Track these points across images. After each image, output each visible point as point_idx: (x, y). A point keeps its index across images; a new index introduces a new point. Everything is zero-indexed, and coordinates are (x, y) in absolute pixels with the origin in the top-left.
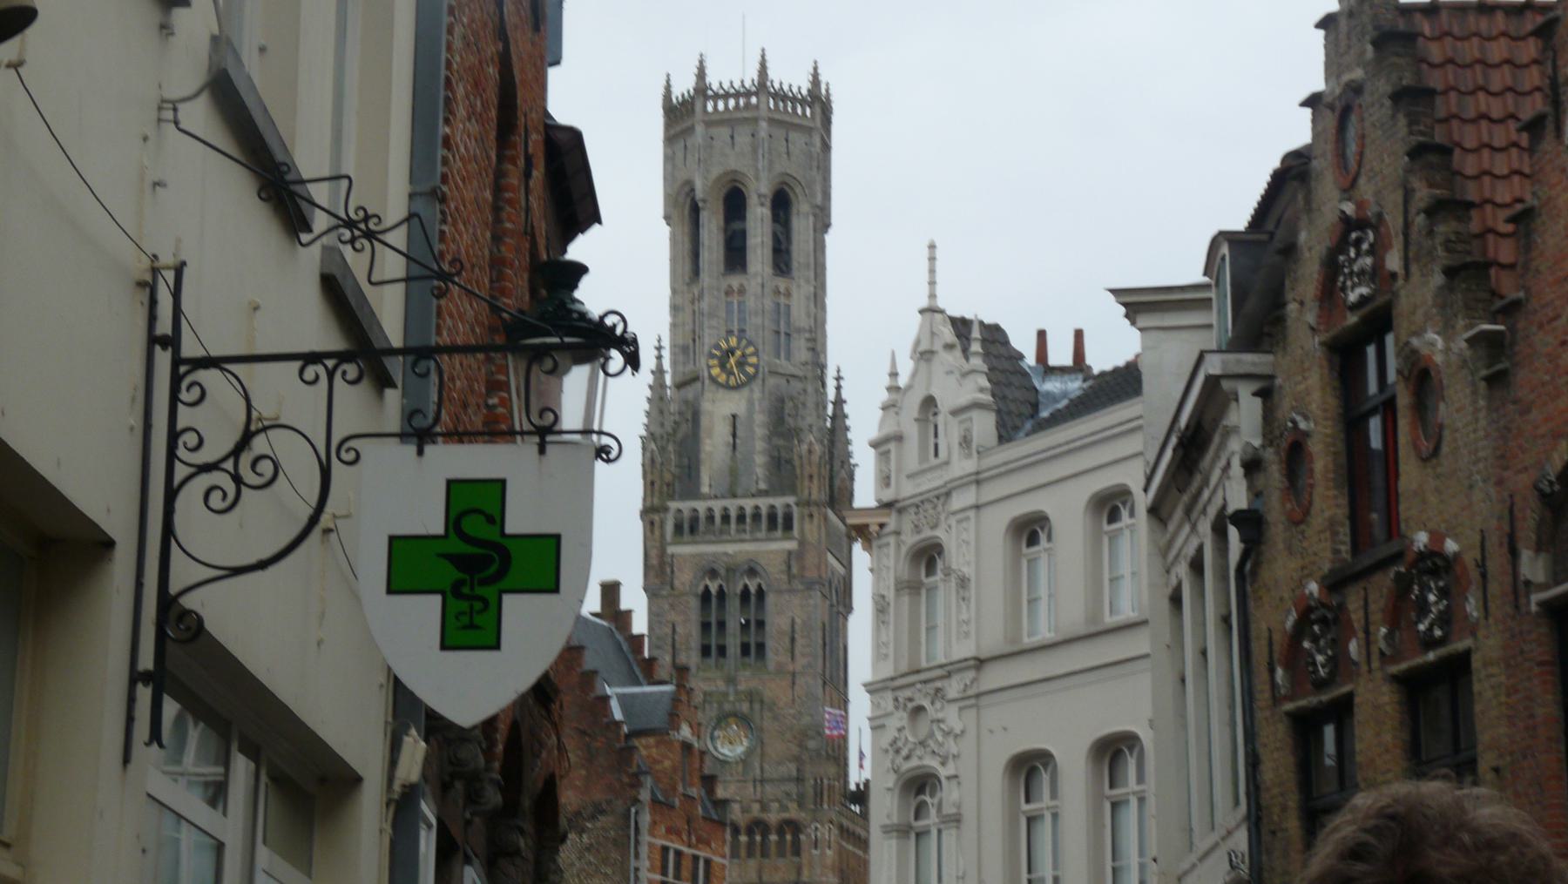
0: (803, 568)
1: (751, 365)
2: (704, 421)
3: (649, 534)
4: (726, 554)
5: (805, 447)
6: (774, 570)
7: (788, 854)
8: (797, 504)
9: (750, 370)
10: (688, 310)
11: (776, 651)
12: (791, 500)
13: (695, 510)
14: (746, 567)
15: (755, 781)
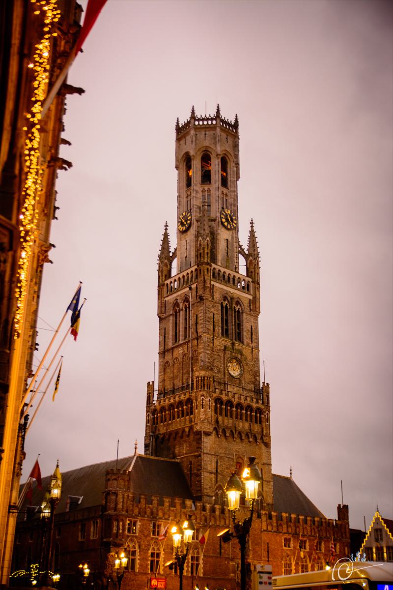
0: (256, 307)
1: (235, 223)
2: (219, 237)
3: (206, 273)
4: (230, 292)
5: (257, 262)
6: (246, 303)
7: (258, 422)
8: (252, 282)
9: (235, 225)
10: (201, 194)
11: (246, 336)
12: (250, 280)
13: (219, 271)
14: (236, 300)
15: (243, 388)
